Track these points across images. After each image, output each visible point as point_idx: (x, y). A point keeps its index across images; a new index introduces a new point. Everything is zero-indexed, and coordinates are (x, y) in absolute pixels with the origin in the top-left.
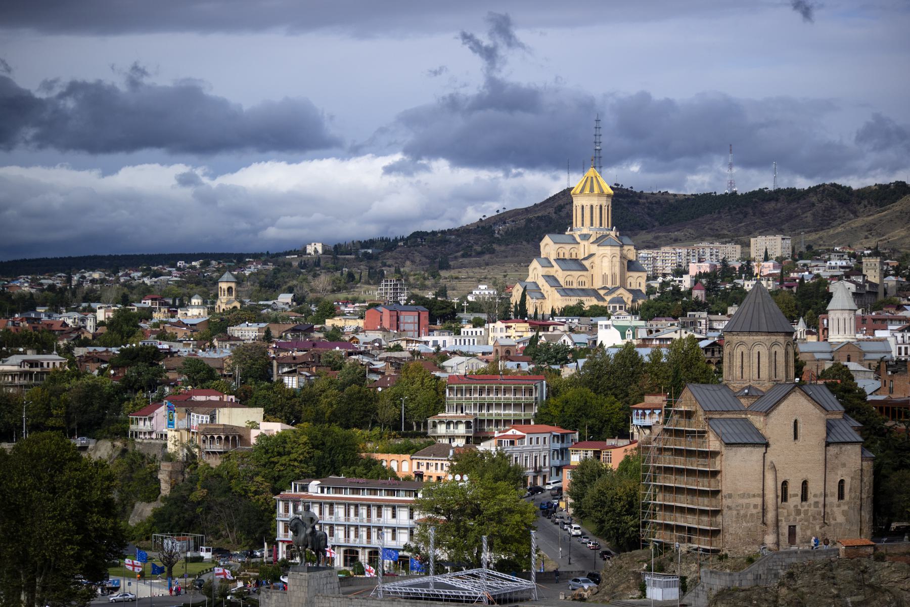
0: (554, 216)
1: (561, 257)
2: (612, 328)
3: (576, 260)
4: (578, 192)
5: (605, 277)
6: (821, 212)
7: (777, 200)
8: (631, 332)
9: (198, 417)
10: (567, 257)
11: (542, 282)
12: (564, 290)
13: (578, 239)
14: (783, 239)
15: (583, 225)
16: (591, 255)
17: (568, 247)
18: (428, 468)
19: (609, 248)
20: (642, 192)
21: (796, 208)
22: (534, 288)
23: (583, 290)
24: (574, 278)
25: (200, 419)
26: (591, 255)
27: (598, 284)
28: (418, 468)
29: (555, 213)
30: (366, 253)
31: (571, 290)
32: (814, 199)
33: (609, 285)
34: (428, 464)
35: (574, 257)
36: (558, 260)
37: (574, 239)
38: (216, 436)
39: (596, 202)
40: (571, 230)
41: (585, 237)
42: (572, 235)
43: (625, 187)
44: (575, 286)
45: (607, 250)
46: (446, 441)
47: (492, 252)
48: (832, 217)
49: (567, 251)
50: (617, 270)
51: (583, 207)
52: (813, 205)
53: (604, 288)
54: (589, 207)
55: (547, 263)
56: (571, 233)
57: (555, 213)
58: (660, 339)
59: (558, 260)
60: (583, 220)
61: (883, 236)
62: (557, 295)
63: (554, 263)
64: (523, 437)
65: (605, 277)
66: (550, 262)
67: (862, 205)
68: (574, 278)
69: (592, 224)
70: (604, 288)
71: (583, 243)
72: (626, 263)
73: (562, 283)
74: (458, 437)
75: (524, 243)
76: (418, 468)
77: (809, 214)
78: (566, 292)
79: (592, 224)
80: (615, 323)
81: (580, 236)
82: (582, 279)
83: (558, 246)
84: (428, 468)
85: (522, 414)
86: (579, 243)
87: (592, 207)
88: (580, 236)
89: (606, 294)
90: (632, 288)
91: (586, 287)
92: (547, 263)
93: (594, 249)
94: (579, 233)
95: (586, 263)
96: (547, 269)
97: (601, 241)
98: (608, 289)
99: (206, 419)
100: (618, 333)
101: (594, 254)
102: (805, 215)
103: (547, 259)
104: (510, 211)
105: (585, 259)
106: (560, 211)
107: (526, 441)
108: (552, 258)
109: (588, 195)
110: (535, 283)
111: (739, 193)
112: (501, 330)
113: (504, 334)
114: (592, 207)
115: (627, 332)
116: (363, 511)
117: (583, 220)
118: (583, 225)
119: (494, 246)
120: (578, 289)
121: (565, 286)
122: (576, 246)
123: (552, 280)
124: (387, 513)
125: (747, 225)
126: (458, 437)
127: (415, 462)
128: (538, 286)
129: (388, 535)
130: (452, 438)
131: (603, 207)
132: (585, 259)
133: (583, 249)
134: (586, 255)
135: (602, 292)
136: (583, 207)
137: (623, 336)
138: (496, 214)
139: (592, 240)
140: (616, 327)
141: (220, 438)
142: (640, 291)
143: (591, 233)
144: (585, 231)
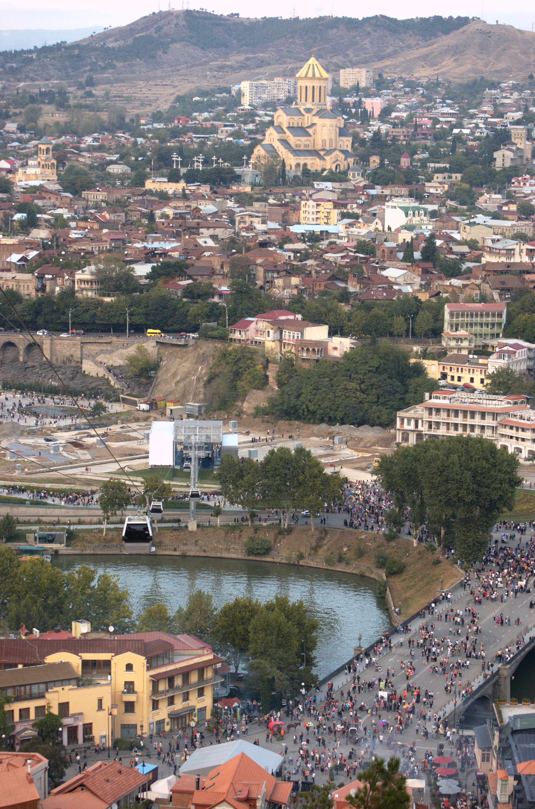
0: (155, 35)
1: (291, 125)
2: (398, 208)
3: (302, 128)
4: (303, 75)
5: (324, 141)
6: (376, 40)
7: (338, 28)
8: (412, 212)
9: (289, 333)
10: (295, 125)
11: (277, 145)
12: (295, 151)
13: (303, 112)
14: (368, 71)
15: (306, 101)
16: (313, 125)
17: (296, 118)
18: (451, 370)
19: (327, 120)
20: (222, 15)
21: (356, 37)
22: (271, 149)
23: (307, 151)
24: (301, 142)
25: (292, 334)
26: (313, 125)
27: (319, 146)
28: (444, 369)
29: (156, 33)
30: (11, 68)
31: (300, 151)
32: (369, 29)
33: (327, 148)
34: (451, 368)
35: (300, 125)
36: (289, 128)
37: (300, 112)
38: (311, 349)
39: (317, 84)
40: (296, 104)
41: (308, 110)
42: (298, 109)
43: (208, 11)
44: (302, 148)
45: (327, 122)
46: (455, 352)
47: (114, 67)
48: (385, 44)
49: (296, 121)
50: (333, 136)
51: (306, 87)
52: (369, 33)
53: (323, 150)
54: (311, 87)
55: (280, 129)
56: (296, 106)
57: (156, 33)
58: (507, 250)
59: (289, 128)
60: (306, 98)
61: (436, 65)
62: (290, 155)
63: (286, 130)
64: (515, 352)
65: (324, 141)
66: (283, 130)
67: (408, 35)
68: (301, 142)
69: (313, 101)
70: (323, 150)
71: (306, 115)
72: (338, 130)
73: (293, 146)
74: (464, 348)
75: (138, 60)
76: (444, 369)
77: (367, 41)
78: (297, 152)
79: (313, 101)
80: (400, 205)
81: (305, 109)
82: (308, 143)
83: (289, 117)
84: (451, 370)
85: (496, 330)
86: (304, 115)
87: (313, 87)
88: (305, 109)
89: (326, 154)
90: (342, 149)
91: (309, 149)
92: (280, 129)
93: (316, 120)
94: (304, 107)
95: (310, 131)
96: (281, 135)
97: (321, 113)
98: (326, 150)
99: (297, 334)
100: (403, 213)
101: (316, 124)
102: (365, 43)
103: (279, 126)
104: (115, 29)
105: (309, 127)
106: (159, 31)
107: (517, 354)
108: (284, 127)
109: (311, 79)
110: (271, 145)
111: (301, 18)
112: (313, 206)
113: (315, 210)
114: (313, 87)
115: (409, 212)
116: (461, 415)
117: (306, 98)
118: (306, 101)
119: (114, 62)
120: (304, 150)
121: (295, 148)
122: (302, 117)
123: (284, 142)
124: (478, 417)
125: (319, 50)
126: (464, 348)
127: (441, 367)
128: (274, 148)
129: (477, 431)
130: (460, 349)
131: (322, 88)
132: (309, 127)
133: (307, 119)
134: (309, 124)
135: (322, 153)
136: (306, 87)
137: (407, 215)
138: (104, 31)
139: (314, 112)
140: (401, 208)
141: (314, 350)
142: (347, 151)
143: (313, 107)
144: (309, 105)
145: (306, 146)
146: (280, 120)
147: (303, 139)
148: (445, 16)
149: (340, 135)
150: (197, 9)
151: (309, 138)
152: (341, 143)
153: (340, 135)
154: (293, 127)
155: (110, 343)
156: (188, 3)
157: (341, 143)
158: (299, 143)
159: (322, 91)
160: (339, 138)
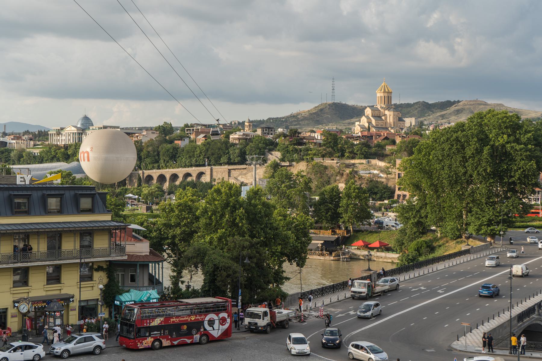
10: (376, 115)
44: (380, 126)
50: (395, 121)
79: (385, 103)
82: (382, 124)
114: (385, 96)
145: (381, 125)
146: (368, 113)
147: (380, 122)
148: (452, 101)
149: (399, 121)
150: (338, 102)
151: (383, 122)
152: (399, 124)
153: (399, 121)
154: (375, 116)
155: (246, 169)
156: (334, 100)
157: (399, 124)
158: (378, 124)
159: (389, 98)
160: (398, 122)
